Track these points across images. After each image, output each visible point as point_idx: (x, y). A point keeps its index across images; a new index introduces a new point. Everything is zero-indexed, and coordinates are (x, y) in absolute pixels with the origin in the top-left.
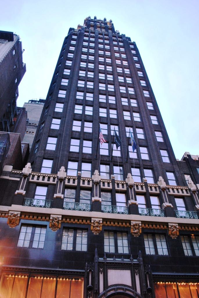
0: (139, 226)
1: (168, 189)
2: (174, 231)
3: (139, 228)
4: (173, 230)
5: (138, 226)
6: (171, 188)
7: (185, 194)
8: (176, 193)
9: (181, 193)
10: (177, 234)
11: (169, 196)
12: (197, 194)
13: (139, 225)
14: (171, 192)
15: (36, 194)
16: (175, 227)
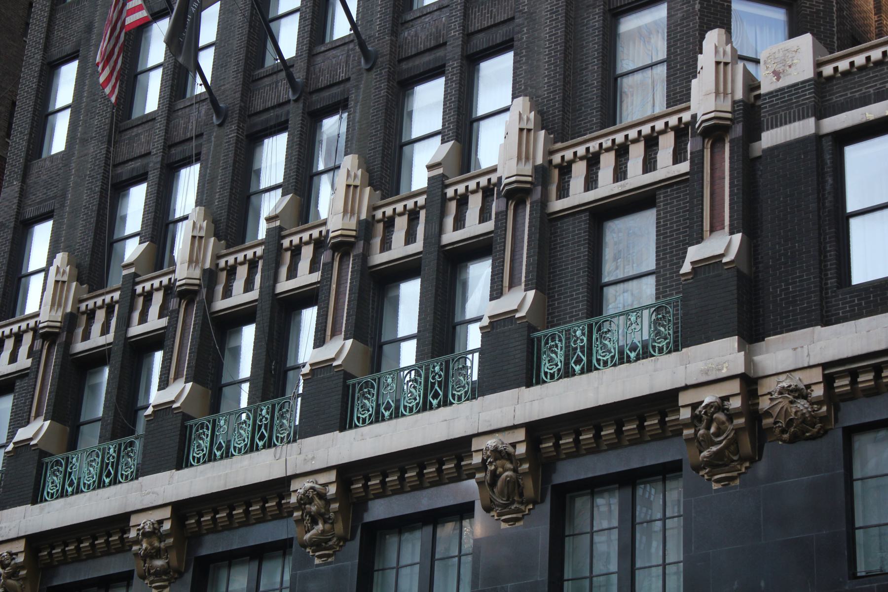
0: (328, 502)
1: (565, 169)
2: (499, 483)
3: (328, 511)
4: (495, 476)
5: (317, 501)
6: (581, 158)
7: (667, 167)
8: (607, 186)
9: (637, 177)
10: (521, 495)
11: (549, 225)
12: (730, 142)
13: (322, 496)
14: (578, 194)
15: (606, 279)
16: (498, 454)
